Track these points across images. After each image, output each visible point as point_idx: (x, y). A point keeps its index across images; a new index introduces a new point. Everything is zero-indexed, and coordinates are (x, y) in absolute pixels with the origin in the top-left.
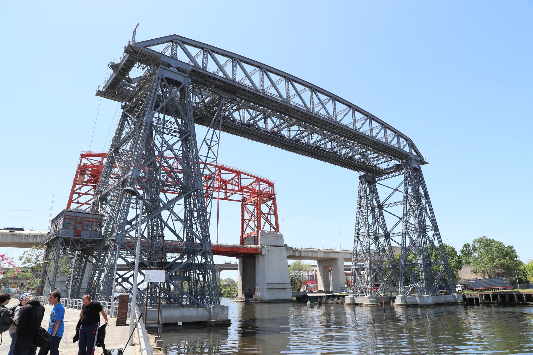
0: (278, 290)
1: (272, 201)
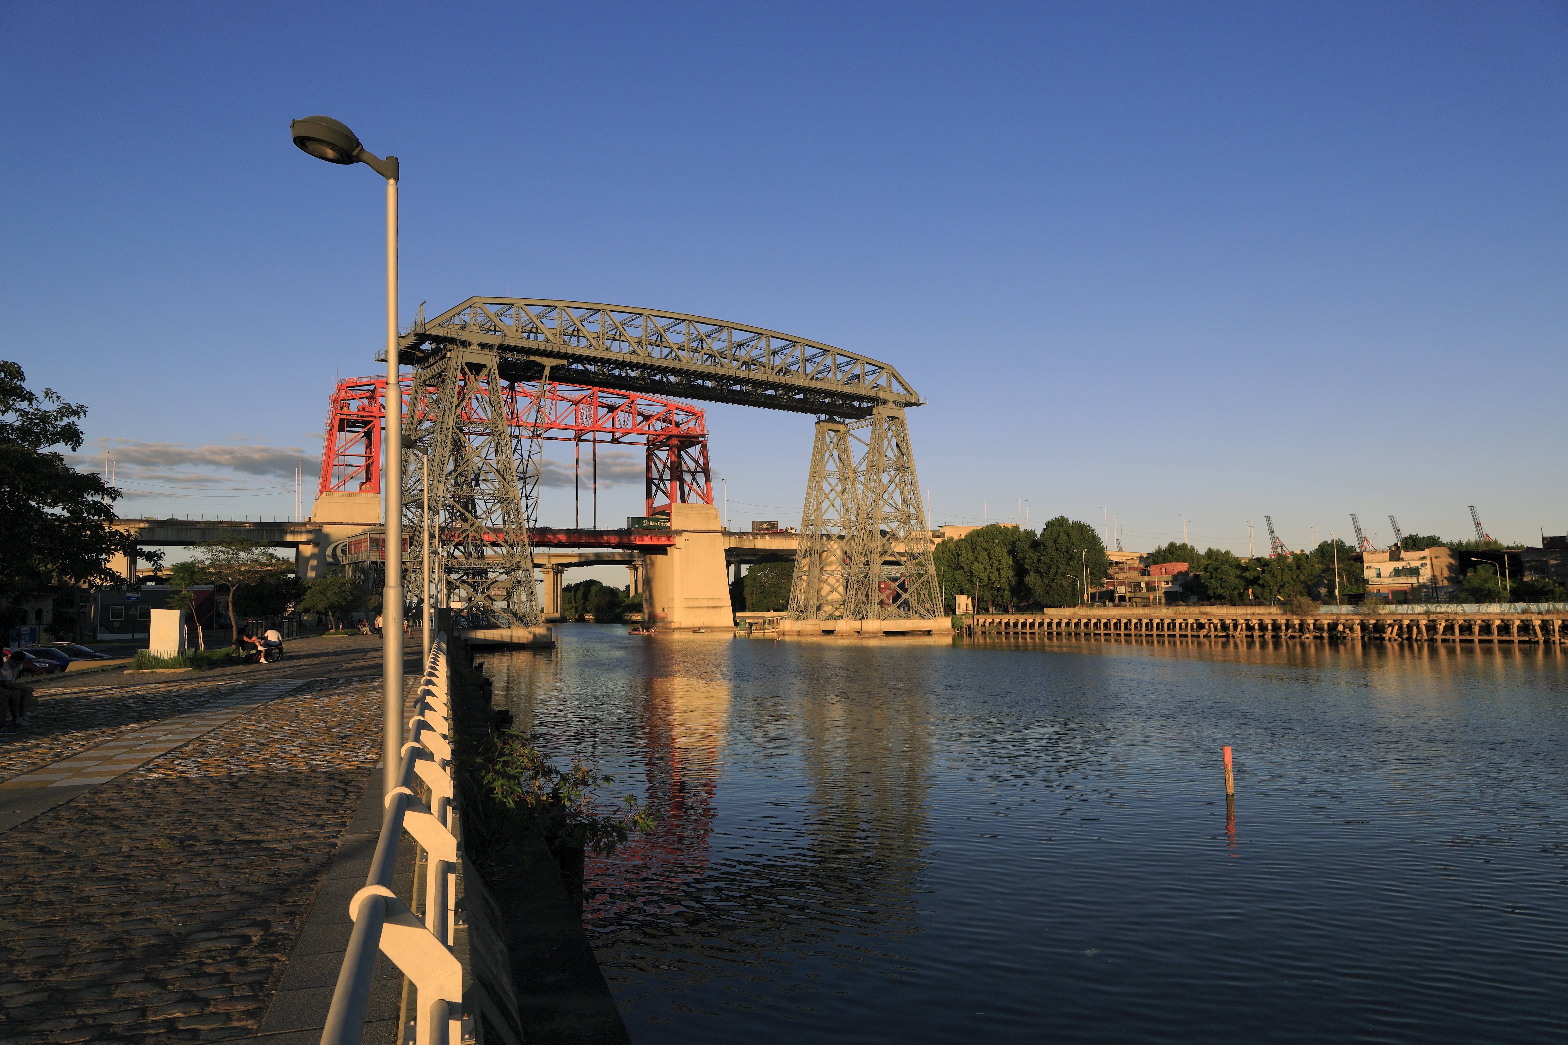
0: (705, 610)
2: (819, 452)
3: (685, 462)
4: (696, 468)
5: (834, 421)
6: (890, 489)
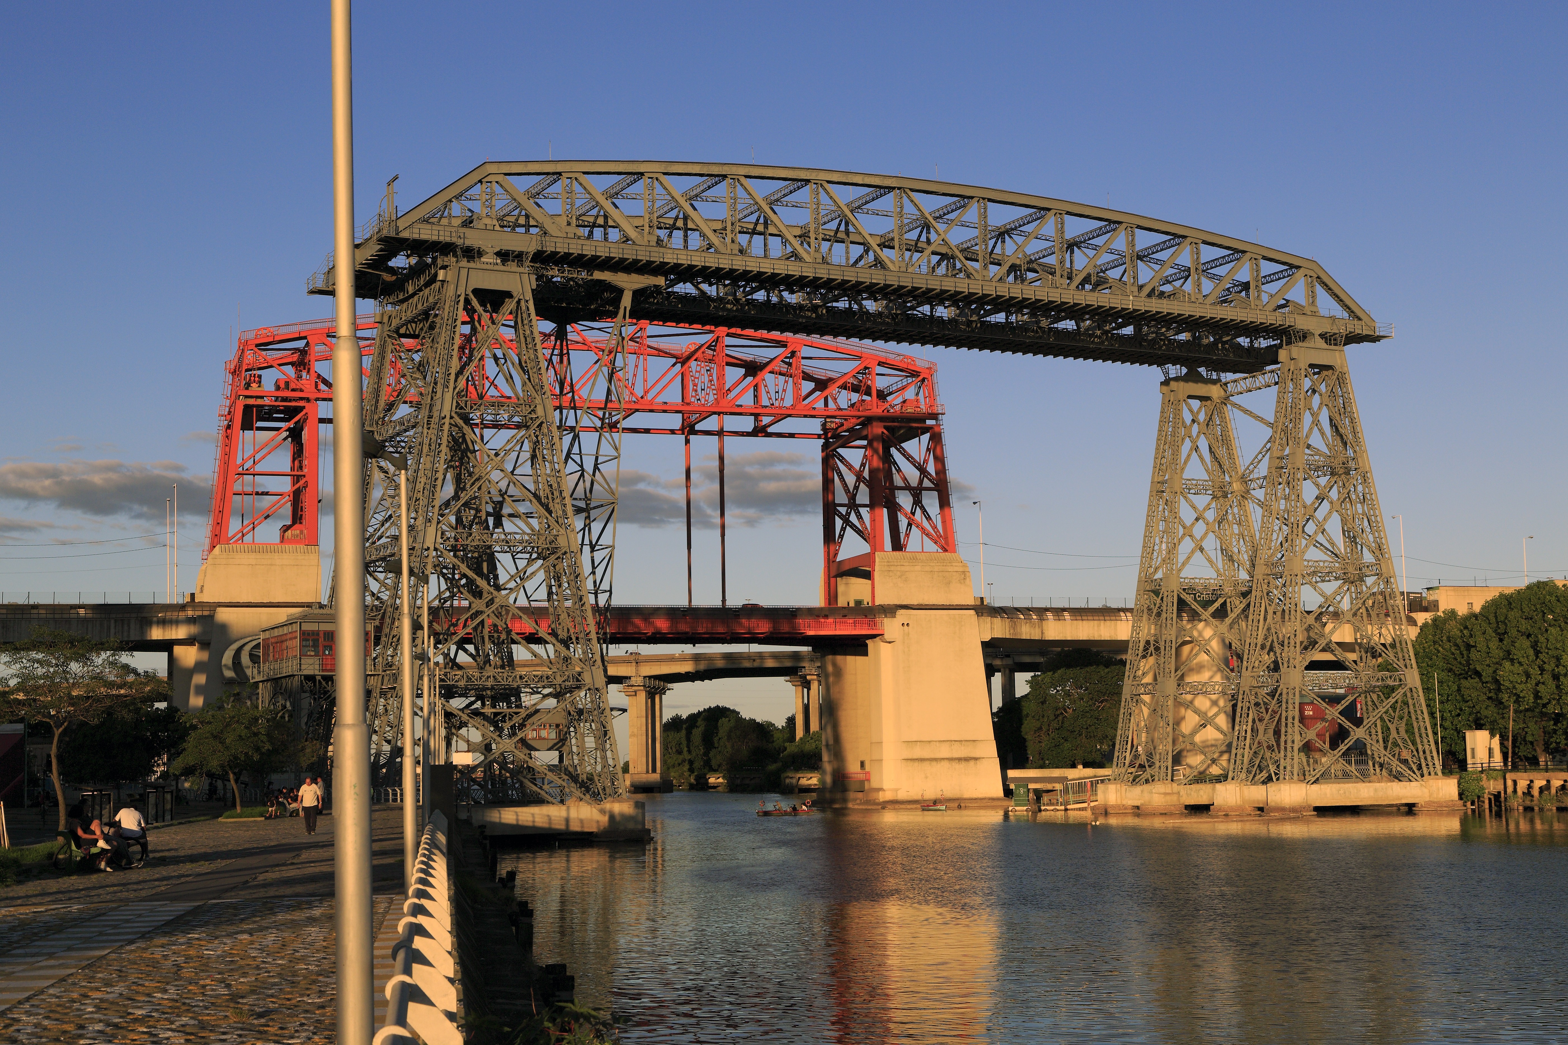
0: (945, 764)
3: (899, 470)
4: (921, 481)
5: (1200, 379)
6: (1320, 514)
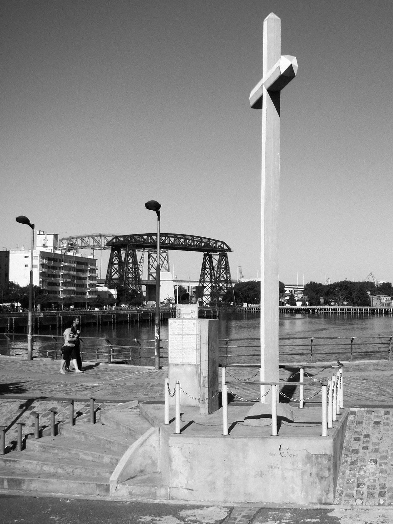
1: (166, 253)
2: (204, 262)
